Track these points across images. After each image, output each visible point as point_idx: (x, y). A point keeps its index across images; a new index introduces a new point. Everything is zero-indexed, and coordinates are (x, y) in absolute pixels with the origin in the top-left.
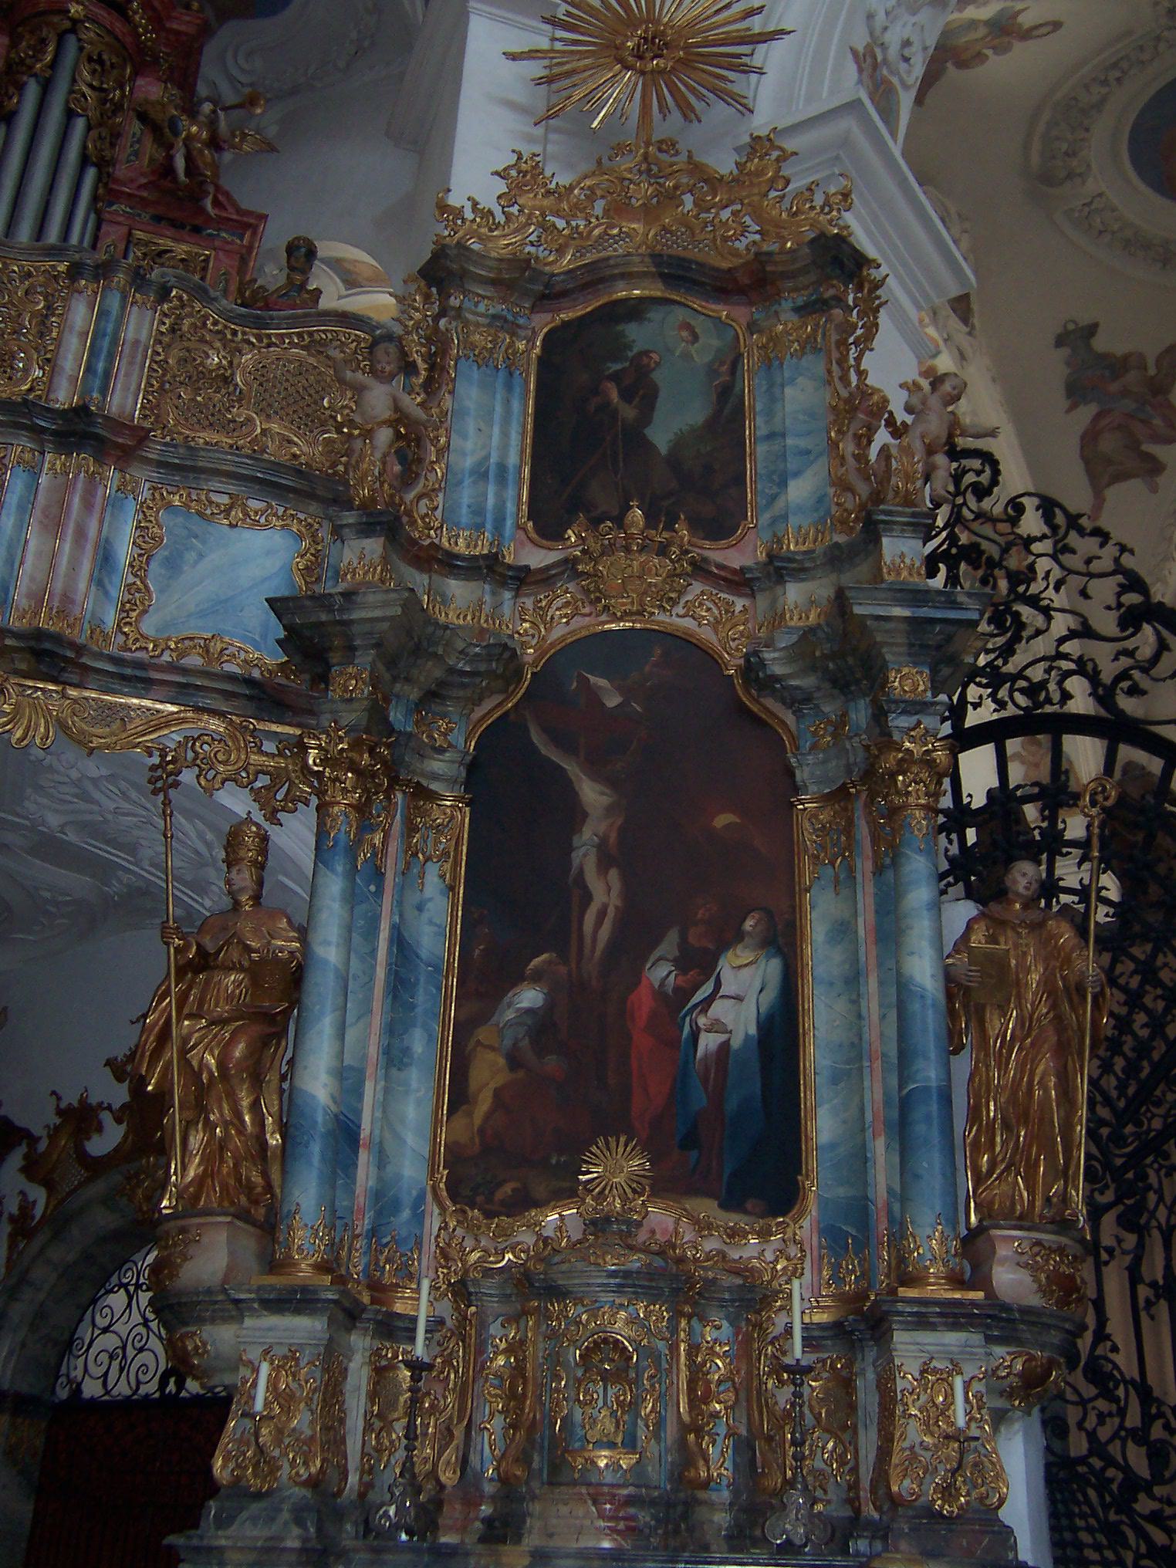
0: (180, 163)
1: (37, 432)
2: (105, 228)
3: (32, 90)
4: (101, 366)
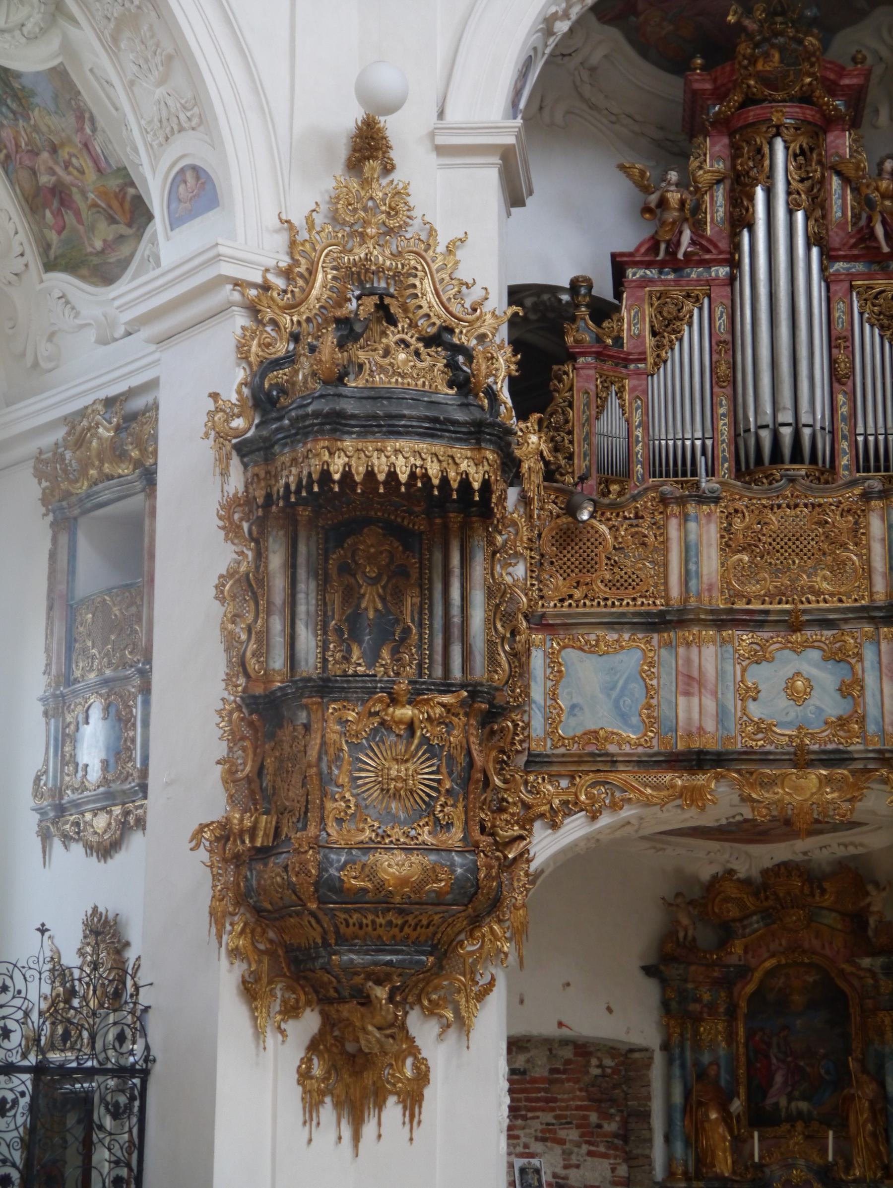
0: (879, 231)
1: (872, 620)
2: (833, 288)
3: (760, 194)
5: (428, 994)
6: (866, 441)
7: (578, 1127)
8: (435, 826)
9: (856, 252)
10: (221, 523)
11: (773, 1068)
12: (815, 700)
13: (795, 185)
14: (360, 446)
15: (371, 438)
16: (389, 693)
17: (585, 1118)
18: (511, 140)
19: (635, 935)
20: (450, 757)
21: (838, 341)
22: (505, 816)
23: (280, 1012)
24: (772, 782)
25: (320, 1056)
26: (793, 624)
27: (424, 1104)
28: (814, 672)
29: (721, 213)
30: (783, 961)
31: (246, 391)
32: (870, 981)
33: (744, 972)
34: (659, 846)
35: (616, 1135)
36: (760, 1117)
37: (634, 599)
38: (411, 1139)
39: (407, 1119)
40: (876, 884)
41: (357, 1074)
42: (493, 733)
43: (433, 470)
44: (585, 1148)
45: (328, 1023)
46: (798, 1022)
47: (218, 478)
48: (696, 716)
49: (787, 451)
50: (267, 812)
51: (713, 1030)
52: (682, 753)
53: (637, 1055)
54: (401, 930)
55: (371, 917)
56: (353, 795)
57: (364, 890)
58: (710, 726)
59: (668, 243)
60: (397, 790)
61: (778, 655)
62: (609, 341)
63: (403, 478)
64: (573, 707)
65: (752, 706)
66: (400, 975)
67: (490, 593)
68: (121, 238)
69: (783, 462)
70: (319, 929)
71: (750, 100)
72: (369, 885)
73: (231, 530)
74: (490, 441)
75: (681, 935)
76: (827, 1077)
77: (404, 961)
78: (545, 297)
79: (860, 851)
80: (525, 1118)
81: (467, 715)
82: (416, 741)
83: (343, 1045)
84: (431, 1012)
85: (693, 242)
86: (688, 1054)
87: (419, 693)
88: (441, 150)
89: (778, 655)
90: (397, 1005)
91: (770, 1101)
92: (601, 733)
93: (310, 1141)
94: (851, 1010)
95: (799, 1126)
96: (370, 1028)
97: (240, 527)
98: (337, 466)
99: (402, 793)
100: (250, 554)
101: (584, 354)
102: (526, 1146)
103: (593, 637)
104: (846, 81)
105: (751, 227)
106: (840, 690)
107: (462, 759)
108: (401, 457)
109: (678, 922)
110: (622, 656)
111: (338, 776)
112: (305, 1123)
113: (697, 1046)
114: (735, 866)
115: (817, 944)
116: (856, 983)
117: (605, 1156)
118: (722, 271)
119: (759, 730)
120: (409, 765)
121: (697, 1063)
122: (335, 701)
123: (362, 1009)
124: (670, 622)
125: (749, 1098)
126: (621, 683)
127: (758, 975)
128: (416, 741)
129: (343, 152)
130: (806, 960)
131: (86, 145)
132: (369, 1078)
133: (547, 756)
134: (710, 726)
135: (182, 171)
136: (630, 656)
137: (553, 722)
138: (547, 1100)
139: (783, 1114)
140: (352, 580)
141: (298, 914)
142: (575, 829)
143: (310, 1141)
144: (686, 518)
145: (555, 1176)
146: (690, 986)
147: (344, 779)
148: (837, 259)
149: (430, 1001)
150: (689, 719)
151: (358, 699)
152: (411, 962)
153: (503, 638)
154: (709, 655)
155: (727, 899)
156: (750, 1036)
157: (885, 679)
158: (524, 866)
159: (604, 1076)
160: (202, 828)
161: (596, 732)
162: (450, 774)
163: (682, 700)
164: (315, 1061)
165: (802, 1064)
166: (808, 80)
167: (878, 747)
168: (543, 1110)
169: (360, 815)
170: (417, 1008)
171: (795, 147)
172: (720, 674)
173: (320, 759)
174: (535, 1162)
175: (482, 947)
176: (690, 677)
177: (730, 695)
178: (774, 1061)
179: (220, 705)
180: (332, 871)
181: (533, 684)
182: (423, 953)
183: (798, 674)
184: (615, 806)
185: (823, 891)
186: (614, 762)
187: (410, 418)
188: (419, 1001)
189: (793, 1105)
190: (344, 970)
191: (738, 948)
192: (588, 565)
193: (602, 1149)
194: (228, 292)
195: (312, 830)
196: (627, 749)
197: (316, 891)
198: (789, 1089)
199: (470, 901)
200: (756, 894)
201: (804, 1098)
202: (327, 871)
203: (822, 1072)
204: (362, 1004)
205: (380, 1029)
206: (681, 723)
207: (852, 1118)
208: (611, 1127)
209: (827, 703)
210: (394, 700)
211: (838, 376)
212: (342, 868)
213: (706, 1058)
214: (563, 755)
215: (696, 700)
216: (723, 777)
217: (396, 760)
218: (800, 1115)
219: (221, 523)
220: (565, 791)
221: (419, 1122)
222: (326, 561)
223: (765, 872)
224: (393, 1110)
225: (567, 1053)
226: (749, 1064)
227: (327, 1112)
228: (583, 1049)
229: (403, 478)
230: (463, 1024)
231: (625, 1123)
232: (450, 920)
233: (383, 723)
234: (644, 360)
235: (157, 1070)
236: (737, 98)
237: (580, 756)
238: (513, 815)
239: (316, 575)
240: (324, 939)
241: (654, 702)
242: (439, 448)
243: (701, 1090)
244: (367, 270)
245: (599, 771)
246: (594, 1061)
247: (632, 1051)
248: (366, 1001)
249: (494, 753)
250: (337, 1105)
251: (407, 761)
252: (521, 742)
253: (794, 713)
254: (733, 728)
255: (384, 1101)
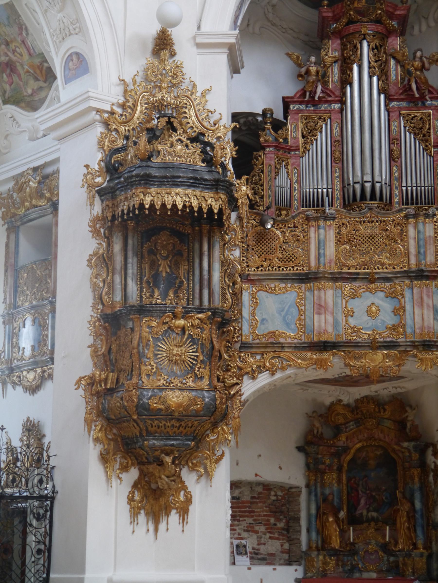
0: (414, 86)
1: (409, 277)
2: (391, 114)
3: (355, 68)
4: (422, 251)
5: (191, 460)
6: (407, 190)
7: (265, 525)
8: (195, 378)
9: (402, 97)
10: (90, 229)
11: (360, 496)
12: (381, 317)
13: (373, 64)
14: (159, 191)
15: (164, 187)
16: (173, 313)
17: (268, 520)
18: (233, 41)
19: (293, 432)
20: (202, 344)
21: (393, 141)
22: (229, 373)
23: (119, 469)
24: (360, 357)
25: (139, 490)
26: (371, 279)
27: (190, 514)
28: (381, 303)
29: (336, 77)
30: (365, 444)
31: (102, 164)
32: (407, 454)
33: (346, 449)
34: (305, 388)
35: (283, 529)
36: (354, 520)
37: (293, 267)
38: (183, 531)
39: (181, 521)
40: (411, 407)
41: (157, 499)
42: (223, 332)
43: (195, 203)
44: (268, 535)
45: (143, 475)
46: (373, 474)
47: (89, 207)
48: (323, 325)
49: (368, 195)
50: (113, 371)
51: (331, 478)
52: (316, 343)
53: (293, 490)
54: (178, 429)
55: (163, 422)
56: (155, 363)
57: (160, 409)
58: (330, 329)
59: (310, 92)
60: (177, 360)
61: (363, 294)
62: (281, 140)
63: (180, 207)
64: (263, 320)
65: (350, 320)
66: (178, 451)
67: (222, 264)
68: (41, 88)
69: (366, 200)
70: (138, 429)
71: (351, 22)
72: (163, 407)
73: (95, 233)
74: (223, 189)
75: (315, 432)
76: (386, 500)
77: (180, 444)
78: (250, 118)
79: (403, 390)
80: (239, 520)
81: (211, 324)
82: (186, 337)
83: (150, 485)
84: (193, 469)
85: (323, 92)
86: (319, 489)
87: (188, 313)
88: (199, 46)
89: (363, 294)
90: (176, 465)
91: (358, 512)
92: (277, 333)
93: (134, 531)
94: (398, 468)
95: (373, 524)
96: (163, 477)
97: (99, 231)
98: (147, 201)
99: (179, 362)
100: (104, 244)
101: (269, 147)
102: (239, 534)
103: (273, 286)
104: (398, 13)
105: (351, 84)
106: (393, 312)
107: (208, 345)
108: (179, 197)
109: (314, 425)
110: (287, 295)
111: (147, 354)
112: (131, 523)
113: (323, 486)
114: (342, 398)
115: (381, 436)
116: (401, 455)
117: (278, 539)
118: (337, 106)
119: (354, 331)
120: (182, 348)
121: (323, 494)
122: (146, 317)
123: (159, 467)
124: (311, 278)
125: (348, 511)
126: (286, 308)
127: (353, 451)
128: (186, 337)
129: (150, 46)
130: (377, 444)
131: (23, 42)
132: (162, 501)
133: (250, 344)
134: (330, 329)
135: (71, 55)
136: (291, 294)
137: (253, 327)
138: (250, 512)
139: (365, 519)
140: (155, 258)
141: (128, 421)
142: (264, 379)
143: (134, 531)
144: (318, 227)
145: (253, 549)
146: (320, 456)
147: (150, 355)
148: (393, 100)
149: (192, 463)
150: (320, 326)
151: (157, 316)
152: (183, 444)
153: (229, 286)
154: (329, 295)
155: (338, 414)
156: (349, 480)
157: (415, 306)
158: (239, 398)
159: (277, 500)
160: (81, 379)
161: (274, 332)
162: (203, 352)
163: (316, 317)
164: (136, 493)
165: (374, 494)
166: (379, 12)
167: (412, 340)
168: (247, 516)
169: (158, 373)
170: (186, 467)
171: (373, 45)
172: (335, 304)
173: (138, 345)
174: (244, 542)
175: (218, 437)
176: (320, 305)
177: (340, 314)
178: (360, 493)
179: (90, 319)
180: (145, 400)
181: (243, 309)
182: (189, 440)
183: (373, 304)
184: (283, 369)
185: (385, 410)
186: (283, 347)
187: (183, 178)
188: (187, 463)
189: (370, 514)
190: (150, 448)
191: (343, 438)
192: (271, 250)
193: (276, 535)
194: (94, 115)
195: (135, 380)
196: (289, 340)
197: (137, 410)
198: (368, 506)
199: (212, 415)
200: (352, 412)
201: (375, 510)
202: (142, 400)
203: (384, 498)
204: (159, 465)
205: (168, 477)
206: (316, 328)
207: (398, 520)
208: (281, 525)
209: (387, 318)
210: (175, 316)
211: (393, 158)
212: (149, 399)
213: (327, 491)
214: (258, 344)
215: (323, 317)
216: (336, 354)
217: (176, 346)
218: (373, 519)
219: (90, 229)
220: (259, 361)
221: (187, 522)
222: (142, 248)
223: (357, 401)
224: (174, 516)
225: (260, 489)
226: (348, 494)
227: (142, 517)
228: (267, 487)
229: (180, 207)
230: (208, 475)
231: (287, 523)
232: (202, 424)
233: (170, 328)
234: (298, 150)
235: (59, 497)
236: (345, 20)
237: (267, 344)
238: (233, 373)
239: (137, 255)
240: (140, 433)
241: (303, 317)
242: (198, 192)
243: (325, 508)
244: (162, 105)
245: (275, 351)
246: (273, 493)
247: (291, 488)
248: (161, 463)
249: (224, 343)
250: (147, 514)
251: (181, 346)
252: (238, 337)
253: (371, 323)
254: (341, 330)
255: (170, 512)
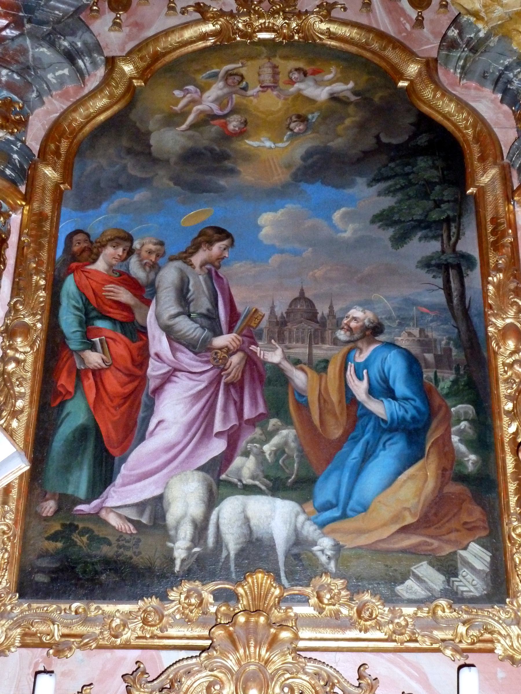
11: (155, 370)
46: (269, 222)
76: (379, 408)
91: (123, 495)
139: (181, 549)
165: (275, 356)
178: (159, 343)
189: (230, 510)
198: (217, 447)
201: (277, 485)
203: (360, 389)
